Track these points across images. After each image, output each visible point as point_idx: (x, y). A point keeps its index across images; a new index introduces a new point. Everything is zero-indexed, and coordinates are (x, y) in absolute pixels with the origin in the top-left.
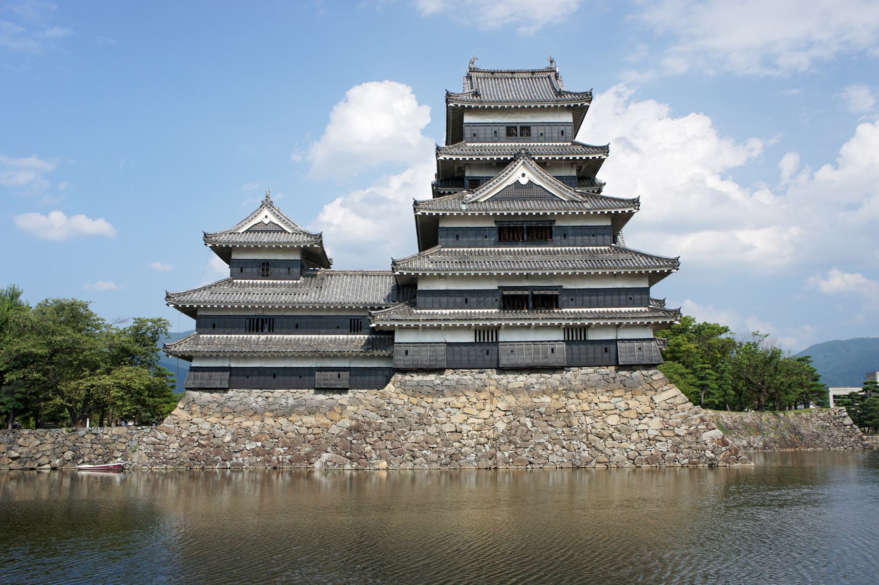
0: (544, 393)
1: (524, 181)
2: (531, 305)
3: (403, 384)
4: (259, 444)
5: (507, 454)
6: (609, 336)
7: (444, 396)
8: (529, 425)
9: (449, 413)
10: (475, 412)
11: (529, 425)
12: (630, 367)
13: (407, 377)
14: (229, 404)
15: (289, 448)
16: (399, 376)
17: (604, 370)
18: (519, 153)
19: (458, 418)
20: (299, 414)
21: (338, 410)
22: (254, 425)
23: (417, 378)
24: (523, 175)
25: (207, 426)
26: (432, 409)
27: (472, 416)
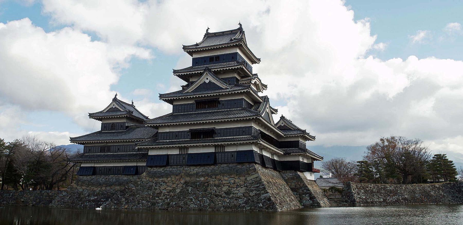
0: (202, 176)
1: (207, 81)
2: (202, 137)
4: (96, 197)
5: (174, 203)
7: (163, 178)
8: (190, 190)
10: (171, 184)
11: (190, 190)
14: (92, 181)
16: (149, 169)
17: (231, 165)
20: (115, 185)
22: (97, 190)
23: (155, 169)
25: (81, 190)
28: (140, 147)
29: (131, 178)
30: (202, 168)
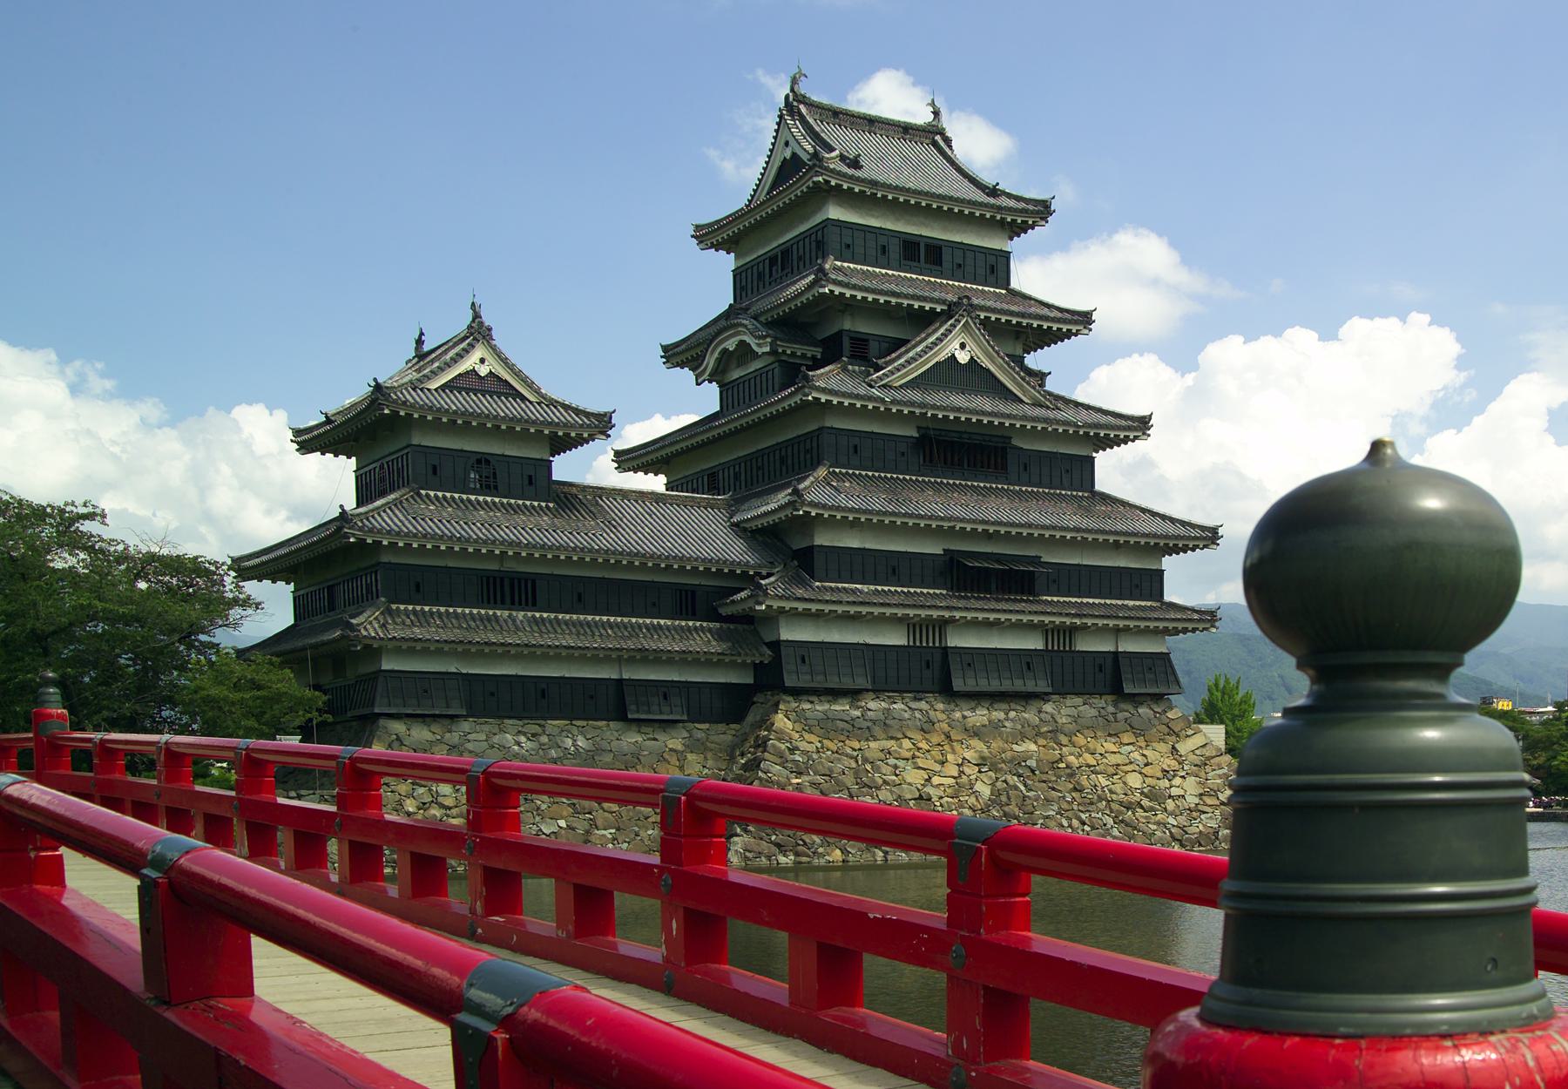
0: (1024, 737)
1: (963, 358)
2: (993, 587)
3: (800, 718)
6: (1106, 646)
9: (896, 767)
12: (1136, 700)
13: (807, 706)
15: (618, 829)
17: (1099, 702)
18: (958, 304)
19: (914, 777)
21: (674, 761)
23: (821, 707)
24: (963, 346)
26: (865, 760)
27: (935, 773)
28: (776, 604)
29: (661, 737)
30: (1005, 706)
